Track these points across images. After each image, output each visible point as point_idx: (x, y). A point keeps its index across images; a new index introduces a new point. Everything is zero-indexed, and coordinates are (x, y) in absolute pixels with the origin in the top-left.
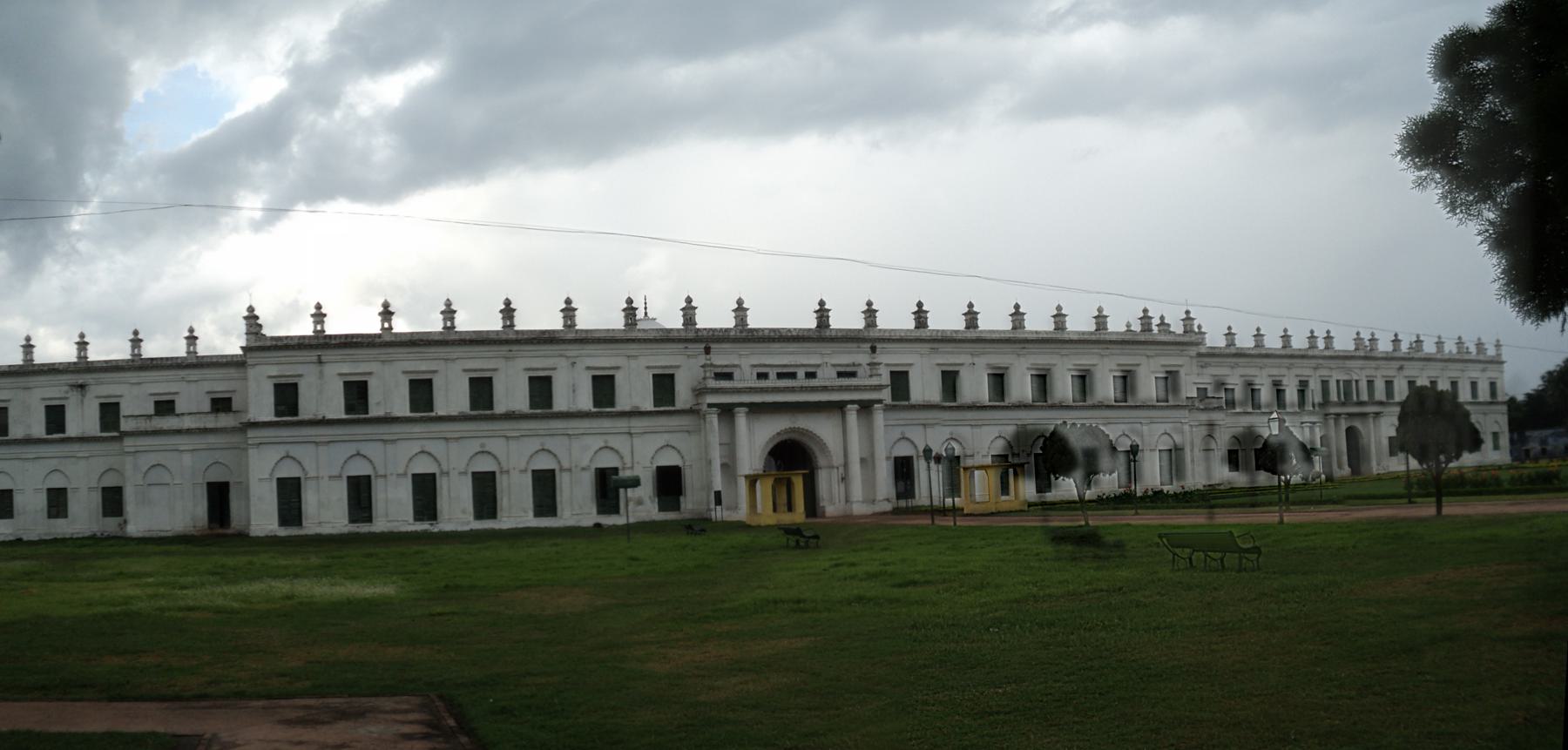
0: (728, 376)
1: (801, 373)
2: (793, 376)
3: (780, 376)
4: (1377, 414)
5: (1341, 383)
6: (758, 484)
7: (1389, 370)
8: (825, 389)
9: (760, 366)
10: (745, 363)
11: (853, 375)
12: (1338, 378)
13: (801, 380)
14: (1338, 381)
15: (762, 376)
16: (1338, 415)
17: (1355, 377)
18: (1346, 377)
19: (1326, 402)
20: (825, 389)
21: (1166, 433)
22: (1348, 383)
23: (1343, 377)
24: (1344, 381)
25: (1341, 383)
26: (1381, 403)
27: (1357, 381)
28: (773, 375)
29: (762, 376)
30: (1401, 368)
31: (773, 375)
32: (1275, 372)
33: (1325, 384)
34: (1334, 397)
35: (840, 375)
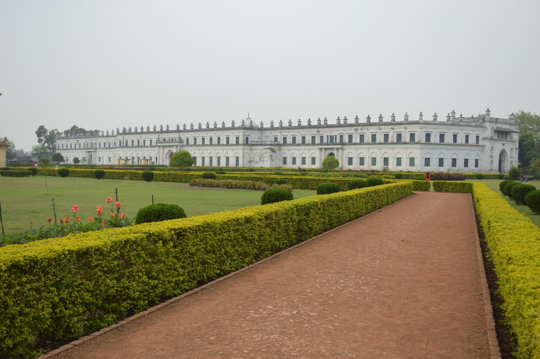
1: (174, 140)
4: (338, 149)
5: (329, 137)
7: (351, 131)
10: (167, 136)
12: (328, 135)
14: (328, 136)
17: (336, 134)
18: (331, 135)
19: (322, 143)
21: (247, 153)
22: (332, 137)
23: (328, 134)
24: (330, 136)
25: (329, 137)
27: (336, 136)
28: (170, 140)
29: (169, 140)
30: (356, 130)
33: (322, 138)
34: (325, 140)
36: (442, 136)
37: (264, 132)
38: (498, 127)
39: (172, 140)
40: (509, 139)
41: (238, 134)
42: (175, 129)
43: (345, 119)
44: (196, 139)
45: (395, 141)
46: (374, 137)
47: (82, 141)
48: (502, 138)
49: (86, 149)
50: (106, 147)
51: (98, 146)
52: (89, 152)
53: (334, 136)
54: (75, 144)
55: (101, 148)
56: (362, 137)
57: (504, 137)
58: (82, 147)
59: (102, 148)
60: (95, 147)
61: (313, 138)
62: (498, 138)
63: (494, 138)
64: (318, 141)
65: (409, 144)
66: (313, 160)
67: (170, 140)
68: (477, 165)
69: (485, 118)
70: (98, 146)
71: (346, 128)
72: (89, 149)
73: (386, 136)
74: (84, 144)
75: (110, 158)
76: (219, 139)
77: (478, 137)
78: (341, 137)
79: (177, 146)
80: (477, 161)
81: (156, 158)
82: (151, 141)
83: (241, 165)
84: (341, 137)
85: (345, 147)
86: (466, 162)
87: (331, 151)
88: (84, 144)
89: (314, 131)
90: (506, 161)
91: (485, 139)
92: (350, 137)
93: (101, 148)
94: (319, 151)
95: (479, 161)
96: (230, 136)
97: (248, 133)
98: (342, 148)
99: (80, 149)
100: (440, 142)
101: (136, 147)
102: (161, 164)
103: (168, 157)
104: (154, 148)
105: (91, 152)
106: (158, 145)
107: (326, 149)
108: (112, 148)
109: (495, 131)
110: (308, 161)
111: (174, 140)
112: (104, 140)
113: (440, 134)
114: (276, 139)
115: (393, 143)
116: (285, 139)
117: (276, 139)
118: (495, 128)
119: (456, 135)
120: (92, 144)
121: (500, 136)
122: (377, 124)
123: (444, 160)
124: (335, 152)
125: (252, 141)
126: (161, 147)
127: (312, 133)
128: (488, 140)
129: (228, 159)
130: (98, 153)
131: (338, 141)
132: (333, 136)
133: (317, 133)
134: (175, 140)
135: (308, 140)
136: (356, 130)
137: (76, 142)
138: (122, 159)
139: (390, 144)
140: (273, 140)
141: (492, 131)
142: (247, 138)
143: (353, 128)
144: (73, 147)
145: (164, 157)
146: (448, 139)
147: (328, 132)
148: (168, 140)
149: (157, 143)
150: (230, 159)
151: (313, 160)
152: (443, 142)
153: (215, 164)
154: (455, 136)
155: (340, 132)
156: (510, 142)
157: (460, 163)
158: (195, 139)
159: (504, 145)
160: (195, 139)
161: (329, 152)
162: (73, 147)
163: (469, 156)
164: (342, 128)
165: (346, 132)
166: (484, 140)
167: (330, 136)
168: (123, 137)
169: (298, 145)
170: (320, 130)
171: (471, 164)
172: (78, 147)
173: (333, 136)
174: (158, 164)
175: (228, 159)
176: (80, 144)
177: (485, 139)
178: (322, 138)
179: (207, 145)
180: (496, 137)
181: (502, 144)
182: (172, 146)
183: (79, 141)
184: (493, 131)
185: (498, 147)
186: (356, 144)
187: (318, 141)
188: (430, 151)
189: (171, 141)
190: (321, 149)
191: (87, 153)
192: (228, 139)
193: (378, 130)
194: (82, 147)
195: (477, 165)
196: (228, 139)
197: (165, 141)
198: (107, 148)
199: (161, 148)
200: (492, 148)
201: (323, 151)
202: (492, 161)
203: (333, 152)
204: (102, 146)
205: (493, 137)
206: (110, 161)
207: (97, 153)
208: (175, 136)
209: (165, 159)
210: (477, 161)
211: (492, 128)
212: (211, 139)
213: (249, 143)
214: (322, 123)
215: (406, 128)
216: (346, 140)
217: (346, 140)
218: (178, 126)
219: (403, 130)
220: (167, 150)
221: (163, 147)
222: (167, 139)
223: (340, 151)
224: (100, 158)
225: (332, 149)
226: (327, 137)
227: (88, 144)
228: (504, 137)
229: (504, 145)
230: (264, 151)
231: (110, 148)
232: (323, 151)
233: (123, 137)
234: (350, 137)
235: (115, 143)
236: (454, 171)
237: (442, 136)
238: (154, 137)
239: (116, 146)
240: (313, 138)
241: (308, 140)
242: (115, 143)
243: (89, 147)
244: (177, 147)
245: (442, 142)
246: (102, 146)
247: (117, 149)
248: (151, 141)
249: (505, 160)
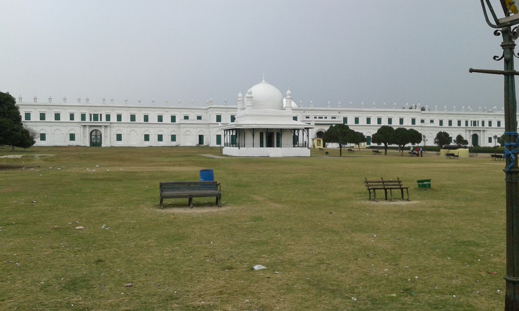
0: (308, 117)
1: (324, 117)
2: (322, 118)
3: (319, 118)
4: (484, 131)
6: (314, 140)
11: (335, 118)
15: (316, 118)
18: (475, 120)
27: (478, 121)
28: (318, 117)
31: (318, 117)
33: (467, 122)
35: (332, 118)
64: (463, 124)
94: (467, 132)
111: (324, 117)
120: (96, 115)
124: (480, 135)
161: (472, 133)
163: (163, 132)
187: (463, 124)
190: (470, 130)
223: (485, 132)
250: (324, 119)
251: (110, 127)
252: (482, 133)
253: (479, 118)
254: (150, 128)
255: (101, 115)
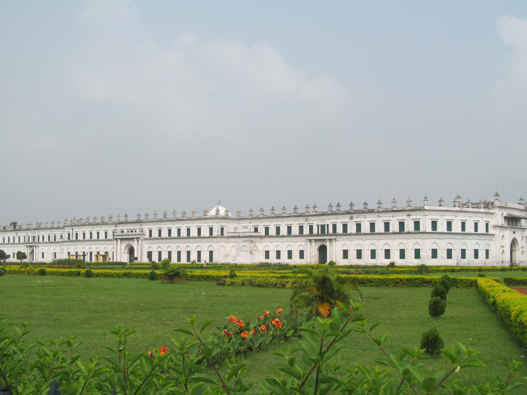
1: (134, 231)
3: (132, 231)
4: (330, 240)
5: (320, 226)
7: (345, 219)
8: (124, 235)
9: (122, 230)
10: (126, 228)
12: (318, 224)
13: (134, 233)
14: (318, 226)
16: (330, 240)
17: (328, 224)
18: (322, 224)
20: (124, 235)
22: (323, 227)
24: (321, 225)
25: (320, 226)
26: (340, 235)
27: (328, 225)
28: (130, 232)
29: (128, 232)
30: (351, 218)
32: (289, 223)
33: (311, 227)
34: (315, 231)
36: (449, 225)
37: (241, 221)
38: (508, 213)
39: (132, 231)
40: (519, 227)
41: (211, 224)
42: (135, 219)
43: (338, 205)
44: (161, 230)
45: (397, 230)
46: (402, 225)
47: (22, 234)
48: (512, 225)
49: (27, 243)
50: (51, 241)
51: (41, 240)
52: (30, 246)
53: (326, 226)
54: (14, 238)
55: (44, 242)
56: (359, 226)
57: (514, 224)
58: (22, 241)
59: (46, 243)
60: (37, 241)
61: (301, 228)
62: (509, 225)
63: (504, 226)
64: (306, 231)
65: (413, 233)
66: (302, 254)
67: (130, 232)
68: (487, 257)
69: (494, 203)
70: (41, 240)
71: (339, 217)
72: (31, 243)
73: (387, 225)
74: (25, 237)
75: (55, 253)
76: (188, 230)
77: (487, 225)
78: (334, 226)
79: (137, 238)
80: (487, 251)
81: (113, 252)
82: (106, 233)
83: (215, 260)
84: (334, 226)
85: (338, 238)
86: (476, 252)
87: (322, 242)
88: (25, 237)
89: (301, 221)
90: (517, 251)
91: (495, 227)
92: (345, 226)
93: (44, 242)
94: (308, 243)
95: (490, 251)
96: (201, 226)
97: (223, 223)
98: (336, 239)
99: (19, 243)
100: (448, 230)
101: (88, 241)
102: (119, 261)
103: (126, 251)
104: (110, 242)
105: (32, 246)
106: (115, 237)
107: (316, 240)
108: (58, 242)
109: (505, 218)
110: (296, 255)
112: (49, 233)
113: (447, 222)
114: (256, 230)
115: (394, 233)
116: (267, 229)
117: (256, 230)
118: (505, 215)
119: (465, 223)
120: (34, 237)
121: (511, 223)
122: (376, 210)
123: (453, 251)
124: (328, 244)
125: (228, 233)
126: (118, 240)
127: (299, 222)
128: (498, 228)
129: (199, 253)
130: (40, 248)
131: (331, 231)
132: (325, 225)
133: (305, 223)
134: (136, 231)
135: (295, 230)
136: (351, 218)
137: (15, 235)
138: (100, 255)
139: (391, 234)
140: (253, 230)
141: (502, 217)
142: (222, 229)
143: (348, 216)
144: (11, 241)
145: (122, 251)
146: (456, 228)
147: (318, 221)
148: (127, 232)
149: (114, 236)
150: (202, 253)
151: (302, 254)
152: (451, 231)
153: (184, 260)
154: (463, 224)
155: (332, 221)
156: (520, 230)
157: (470, 254)
158: (160, 231)
159: (514, 233)
160: (160, 231)
161: (319, 244)
162: (11, 241)
164: (335, 217)
165: (340, 221)
166: (494, 228)
167: (321, 225)
168: (73, 229)
169: (283, 236)
170: (309, 218)
171: (482, 254)
172: (17, 241)
173: (325, 225)
174: (115, 261)
175: (199, 253)
176: (19, 238)
177: (495, 227)
178: (311, 227)
179: (174, 238)
180: (506, 225)
181: (512, 233)
182: (132, 239)
183: (18, 234)
184: (503, 218)
185: (508, 235)
186: (351, 235)
187: (306, 231)
188: (437, 241)
189: (130, 233)
190: (310, 240)
191: (29, 248)
192: (199, 230)
193: (377, 218)
194: (22, 241)
195: (487, 257)
196: (199, 230)
197: (123, 234)
198: (51, 243)
199: (119, 242)
200: (503, 236)
201: (313, 243)
202: (503, 251)
203: (324, 243)
204: (46, 239)
205: (503, 224)
206: (55, 257)
207: (39, 248)
208: (137, 227)
209: (123, 255)
210: (487, 251)
211: (502, 214)
212: (179, 230)
213: (225, 234)
214: (311, 210)
215: (408, 215)
216: (340, 230)
217: (340, 230)
218: (139, 215)
219: (406, 217)
220: (124, 244)
221: (121, 239)
222: (125, 232)
223: (334, 242)
224: (43, 253)
225: (324, 240)
226: (317, 226)
227: (29, 237)
228: (514, 224)
229: (514, 233)
230: (242, 244)
231: (55, 242)
232: (313, 243)
233: (73, 229)
234: (345, 226)
235: (61, 236)
236: (464, 263)
237: (449, 225)
238: (110, 230)
239: (63, 240)
240: (301, 228)
241: (295, 230)
242: (61, 236)
243: (31, 241)
244: (138, 241)
245: (449, 231)
246: (46, 239)
247: (65, 243)
248: (106, 233)
249: (516, 250)
250: (134, 233)
251: (38, 247)
252: (328, 243)
253: (327, 220)
254: (213, 243)
255: (39, 237)
